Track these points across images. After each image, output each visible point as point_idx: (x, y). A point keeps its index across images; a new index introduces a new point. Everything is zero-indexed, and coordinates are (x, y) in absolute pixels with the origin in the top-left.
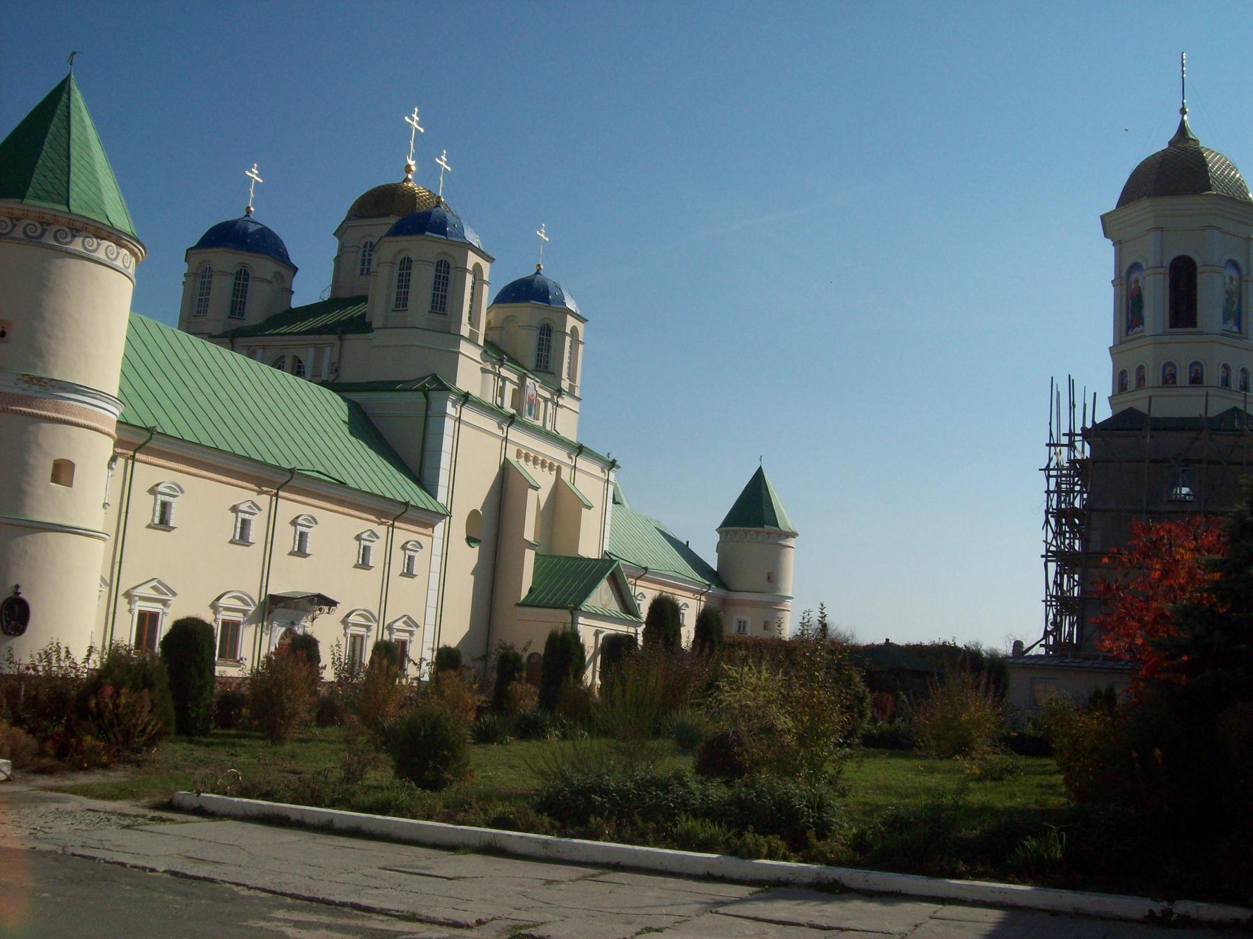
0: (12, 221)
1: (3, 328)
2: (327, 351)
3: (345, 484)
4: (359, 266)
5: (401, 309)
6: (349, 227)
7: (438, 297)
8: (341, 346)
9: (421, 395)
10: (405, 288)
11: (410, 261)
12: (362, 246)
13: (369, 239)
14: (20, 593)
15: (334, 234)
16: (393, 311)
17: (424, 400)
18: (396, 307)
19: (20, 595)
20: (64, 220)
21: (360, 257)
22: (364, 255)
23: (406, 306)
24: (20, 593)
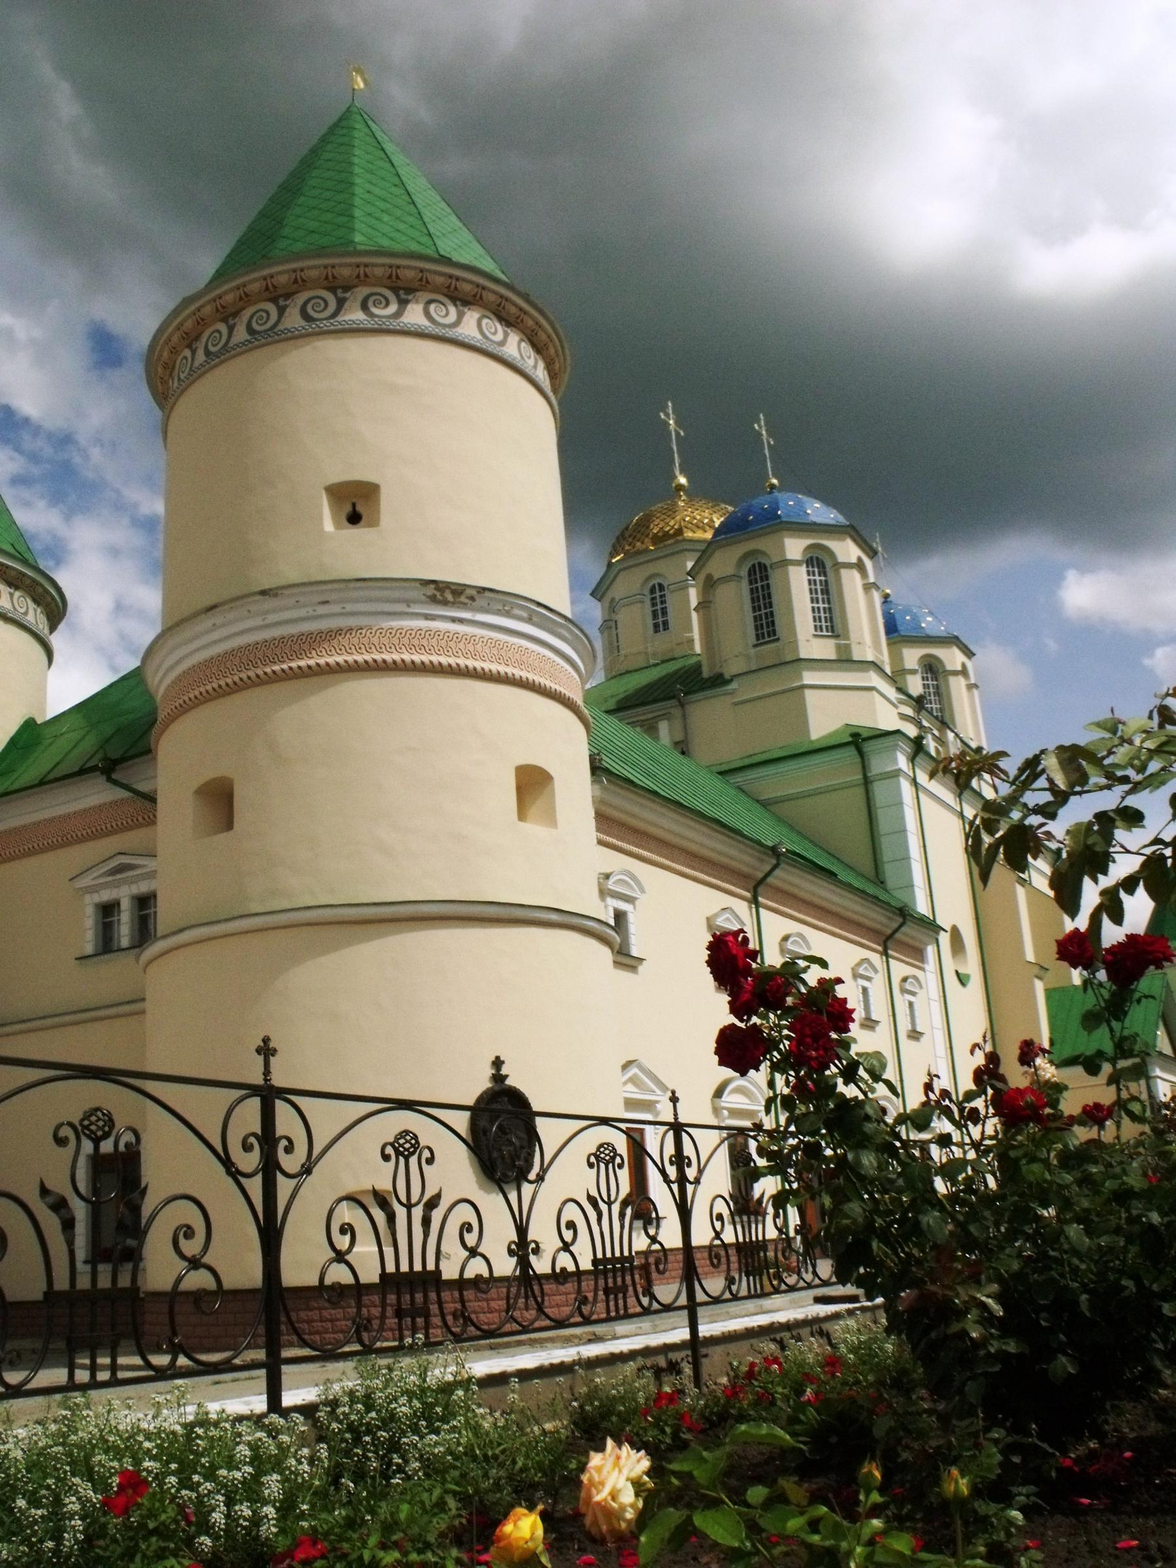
0: (335, 294)
1: (354, 505)
2: (663, 727)
3: (835, 875)
4: (650, 622)
5: (767, 639)
6: (620, 571)
7: (819, 612)
8: (684, 717)
9: (851, 752)
10: (760, 615)
11: (763, 568)
12: (647, 592)
13: (655, 581)
14: (507, 1076)
15: (592, 594)
16: (755, 646)
17: (858, 760)
18: (758, 639)
19: (508, 1082)
20: (440, 280)
21: (648, 609)
22: (654, 605)
23: (775, 635)
24: (507, 1076)
